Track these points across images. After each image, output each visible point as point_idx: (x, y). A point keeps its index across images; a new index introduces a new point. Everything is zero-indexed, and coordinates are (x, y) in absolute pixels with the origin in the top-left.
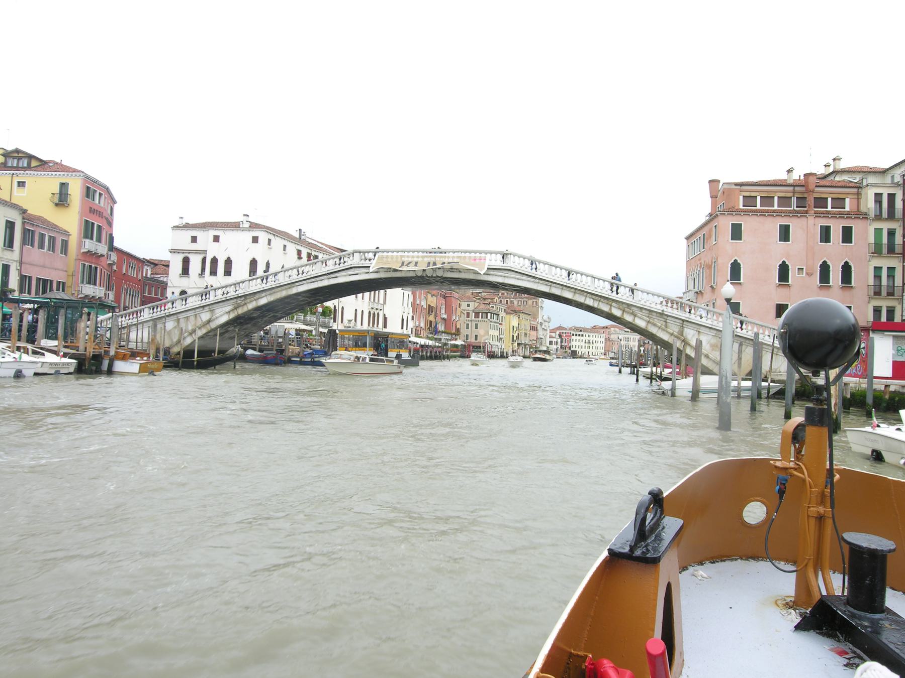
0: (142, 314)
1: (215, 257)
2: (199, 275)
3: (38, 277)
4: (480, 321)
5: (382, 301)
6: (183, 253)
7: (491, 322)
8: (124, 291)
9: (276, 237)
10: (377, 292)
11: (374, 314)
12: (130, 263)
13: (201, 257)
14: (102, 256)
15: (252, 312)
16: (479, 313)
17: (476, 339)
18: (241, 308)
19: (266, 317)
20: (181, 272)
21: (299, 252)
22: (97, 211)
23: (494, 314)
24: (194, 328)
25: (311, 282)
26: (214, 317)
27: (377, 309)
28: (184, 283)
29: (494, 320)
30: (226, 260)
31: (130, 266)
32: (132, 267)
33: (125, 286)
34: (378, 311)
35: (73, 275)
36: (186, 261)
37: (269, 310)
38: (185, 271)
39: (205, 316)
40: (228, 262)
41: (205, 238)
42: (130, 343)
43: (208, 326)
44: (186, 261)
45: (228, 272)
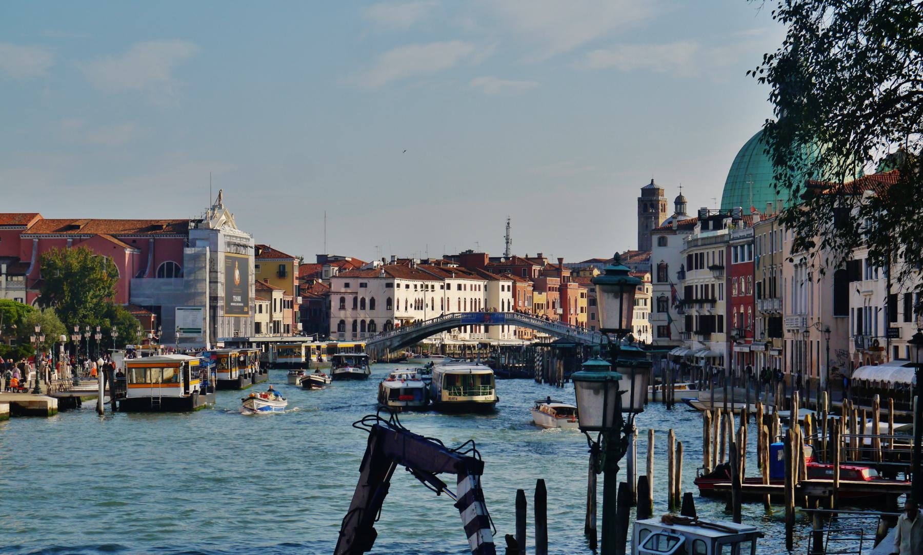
13: (352, 296)
28: (342, 314)
36: (343, 300)
38: (342, 307)
40: (373, 301)
41: (354, 283)
44: (343, 300)
45: (372, 306)
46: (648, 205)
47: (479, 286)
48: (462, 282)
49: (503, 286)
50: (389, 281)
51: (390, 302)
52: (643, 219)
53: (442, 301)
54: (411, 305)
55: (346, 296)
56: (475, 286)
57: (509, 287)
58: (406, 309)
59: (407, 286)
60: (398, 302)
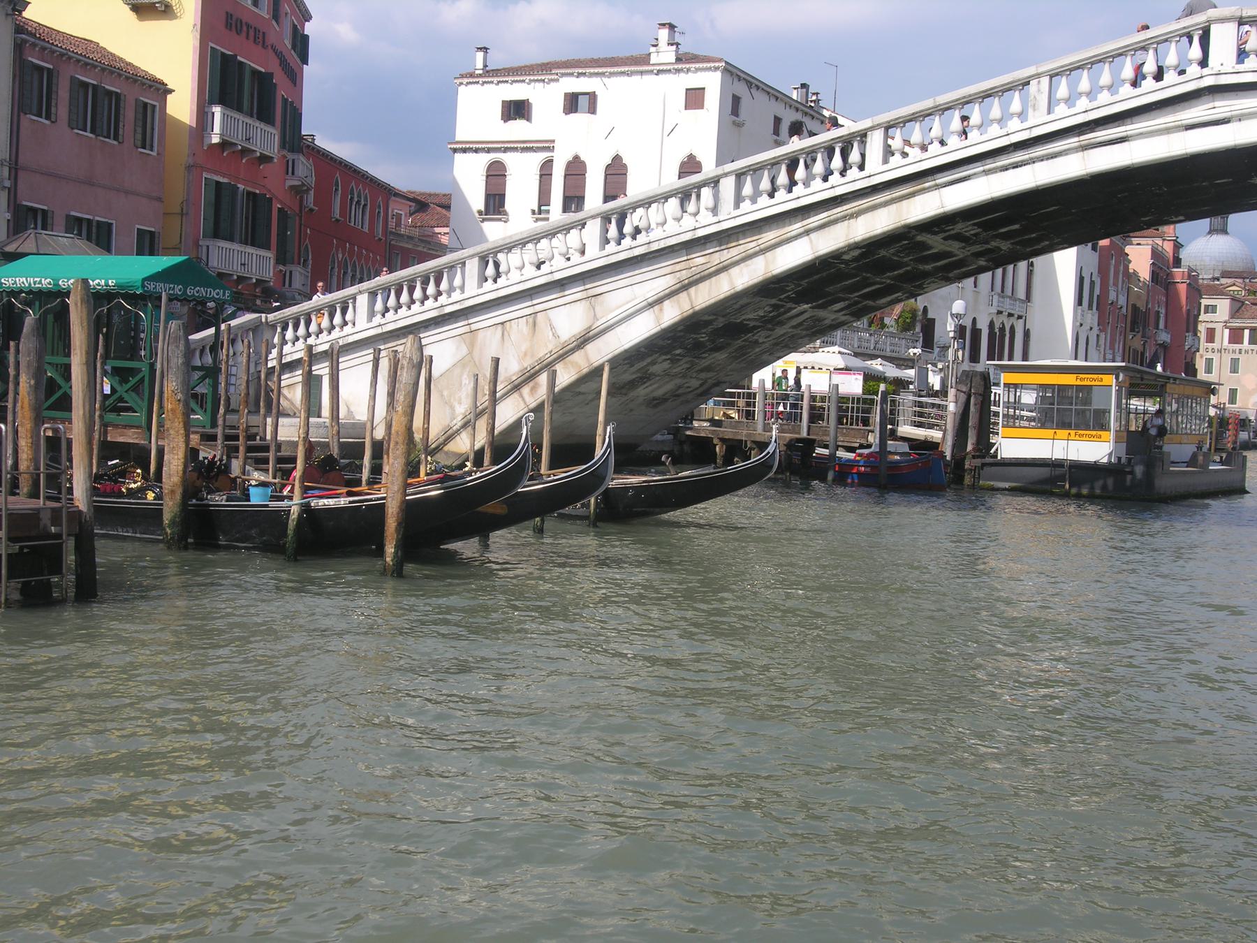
0: (349, 317)
1: (576, 158)
2: (533, 212)
3: (73, 213)
4: (1247, 352)
5: (1021, 294)
6: (489, 151)
8: (336, 270)
9: (754, 91)
10: (1010, 267)
11: (1002, 329)
12: (352, 193)
14: (265, 159)
15: (744, 301)
16: (1243, 329)
17: (1233, 399)
18: (703, 286)
19: (781, 323)
22: (248, 26)
24: (528, 363)
25: (1005, 168)
26: (601, 323)
27: (1010, 315)
30: (608, 167)
31: (352, 199)
32: (358, 202)
33: (340, 256)
34: (1013, 320)
35: (182, 215)
37: (801, 297)
40: (616, 173)
42: (281, 420)
43: (577, 357)
55: (508, 159)
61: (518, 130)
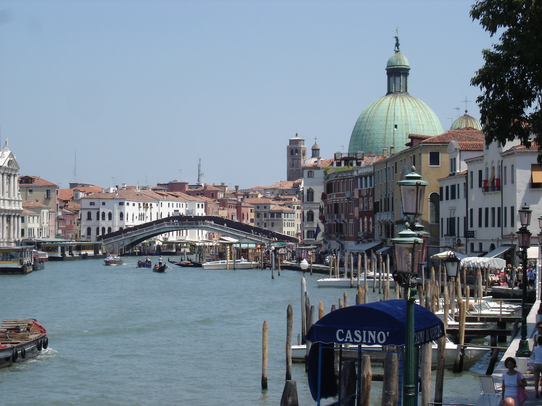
1: (103, 212)
4: (276, 220)
7: (285, 220)
13: (96, 212)
20: (87, 218)
21: (139, 204)
23: (288, 213)
28: (90, 223)
29: (289, 218)
30: (109, 214)
36: (89, 214)
38: (89, 218)
39: (121, 243)
40: (110, 215)
44: (89, 214)
46: (294, 151)
47: (182, 204)
48: (171, 203)
49: (198, 205)
50: (121, 201)
51: (122, 215)
52: (290, 160)
53: (157, 214)
54: (136, 217)
56: (180, 204)
57: (202, 205)
58: (133, 220)
59: (134, 205)
60: (127, 215)
61: (92, 207)
